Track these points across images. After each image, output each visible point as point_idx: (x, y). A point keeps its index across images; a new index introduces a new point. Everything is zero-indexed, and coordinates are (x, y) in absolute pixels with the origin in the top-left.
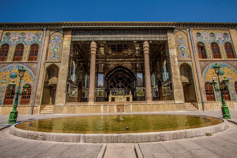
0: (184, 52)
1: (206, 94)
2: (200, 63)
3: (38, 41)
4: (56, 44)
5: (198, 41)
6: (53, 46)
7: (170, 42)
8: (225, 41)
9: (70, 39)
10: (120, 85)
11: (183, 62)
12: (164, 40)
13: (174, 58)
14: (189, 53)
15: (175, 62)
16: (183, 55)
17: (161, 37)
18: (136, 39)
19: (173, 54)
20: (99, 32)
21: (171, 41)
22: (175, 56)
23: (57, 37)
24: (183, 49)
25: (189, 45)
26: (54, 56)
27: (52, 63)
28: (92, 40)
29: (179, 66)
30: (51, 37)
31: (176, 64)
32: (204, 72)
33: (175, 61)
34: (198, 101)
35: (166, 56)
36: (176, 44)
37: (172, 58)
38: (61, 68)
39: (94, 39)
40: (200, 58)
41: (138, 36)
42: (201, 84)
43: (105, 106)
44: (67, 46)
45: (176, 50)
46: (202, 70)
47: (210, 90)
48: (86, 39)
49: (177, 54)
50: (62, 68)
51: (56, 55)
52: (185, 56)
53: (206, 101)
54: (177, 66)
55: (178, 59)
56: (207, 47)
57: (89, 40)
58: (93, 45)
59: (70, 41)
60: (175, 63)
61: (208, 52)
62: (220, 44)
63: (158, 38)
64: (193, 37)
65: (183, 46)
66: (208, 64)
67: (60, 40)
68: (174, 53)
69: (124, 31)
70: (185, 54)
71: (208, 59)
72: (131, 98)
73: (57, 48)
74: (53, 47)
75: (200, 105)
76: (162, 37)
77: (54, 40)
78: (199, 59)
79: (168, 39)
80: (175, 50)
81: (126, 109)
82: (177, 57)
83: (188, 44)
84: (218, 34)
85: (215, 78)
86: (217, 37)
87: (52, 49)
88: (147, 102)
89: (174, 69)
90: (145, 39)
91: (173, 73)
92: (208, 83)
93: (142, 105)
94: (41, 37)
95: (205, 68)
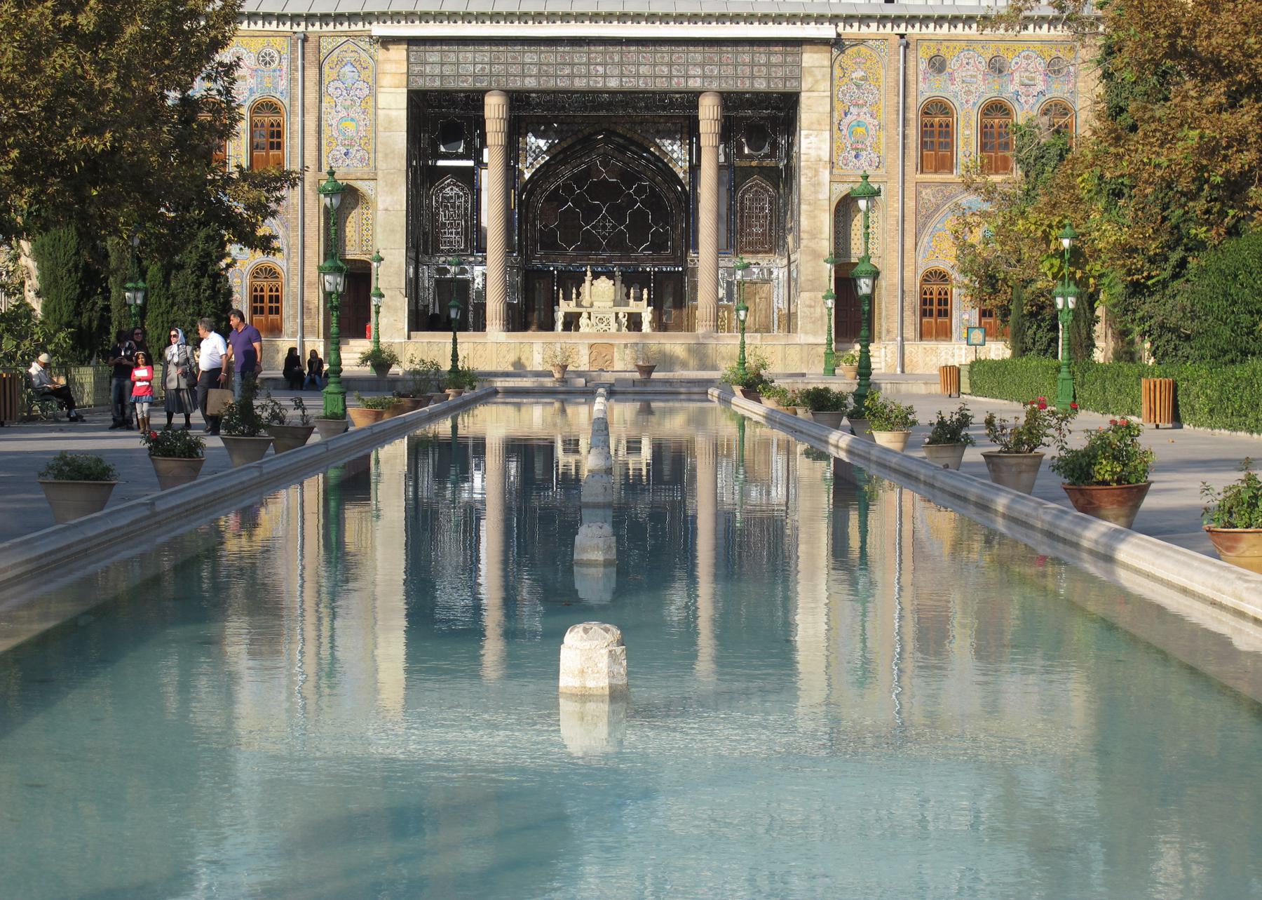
1: (918, 313)
4: (349, 102)
5: (927, 95)
6: (339, 108)
7: (809, 98)
8: (1047, 97)
9: (405, 83)
12: (787, 90)
13: (816, 171)
15: (816, 185)
17: (774, 75)
19: (813, 153)
21: (815, 94)
22: (820, 160)
23: (348, 68)
30: (326, 69)
31: (821, 197)
33: (819, 184)
37: (809, 168)
38: (381, 206)
44: (394, 113)
48: (466, 81)
51: (353, 151)
52: (862, 161)
56: (961, 124)
57: (478, 85)
60: (816, 192)
61: (961, 143)
62: (1022, 109)
65: (862, 118)
68: (820, 149)
70: (864, 153)
72: (647, 314)
73: (352, 119)
79: (804, 86)
84: (1025, 62)
86: (1017, 76)
87: (334, 122)
89: (813, 217)
91: (804, 232)
92: (936, 272)
94: (285, 69)
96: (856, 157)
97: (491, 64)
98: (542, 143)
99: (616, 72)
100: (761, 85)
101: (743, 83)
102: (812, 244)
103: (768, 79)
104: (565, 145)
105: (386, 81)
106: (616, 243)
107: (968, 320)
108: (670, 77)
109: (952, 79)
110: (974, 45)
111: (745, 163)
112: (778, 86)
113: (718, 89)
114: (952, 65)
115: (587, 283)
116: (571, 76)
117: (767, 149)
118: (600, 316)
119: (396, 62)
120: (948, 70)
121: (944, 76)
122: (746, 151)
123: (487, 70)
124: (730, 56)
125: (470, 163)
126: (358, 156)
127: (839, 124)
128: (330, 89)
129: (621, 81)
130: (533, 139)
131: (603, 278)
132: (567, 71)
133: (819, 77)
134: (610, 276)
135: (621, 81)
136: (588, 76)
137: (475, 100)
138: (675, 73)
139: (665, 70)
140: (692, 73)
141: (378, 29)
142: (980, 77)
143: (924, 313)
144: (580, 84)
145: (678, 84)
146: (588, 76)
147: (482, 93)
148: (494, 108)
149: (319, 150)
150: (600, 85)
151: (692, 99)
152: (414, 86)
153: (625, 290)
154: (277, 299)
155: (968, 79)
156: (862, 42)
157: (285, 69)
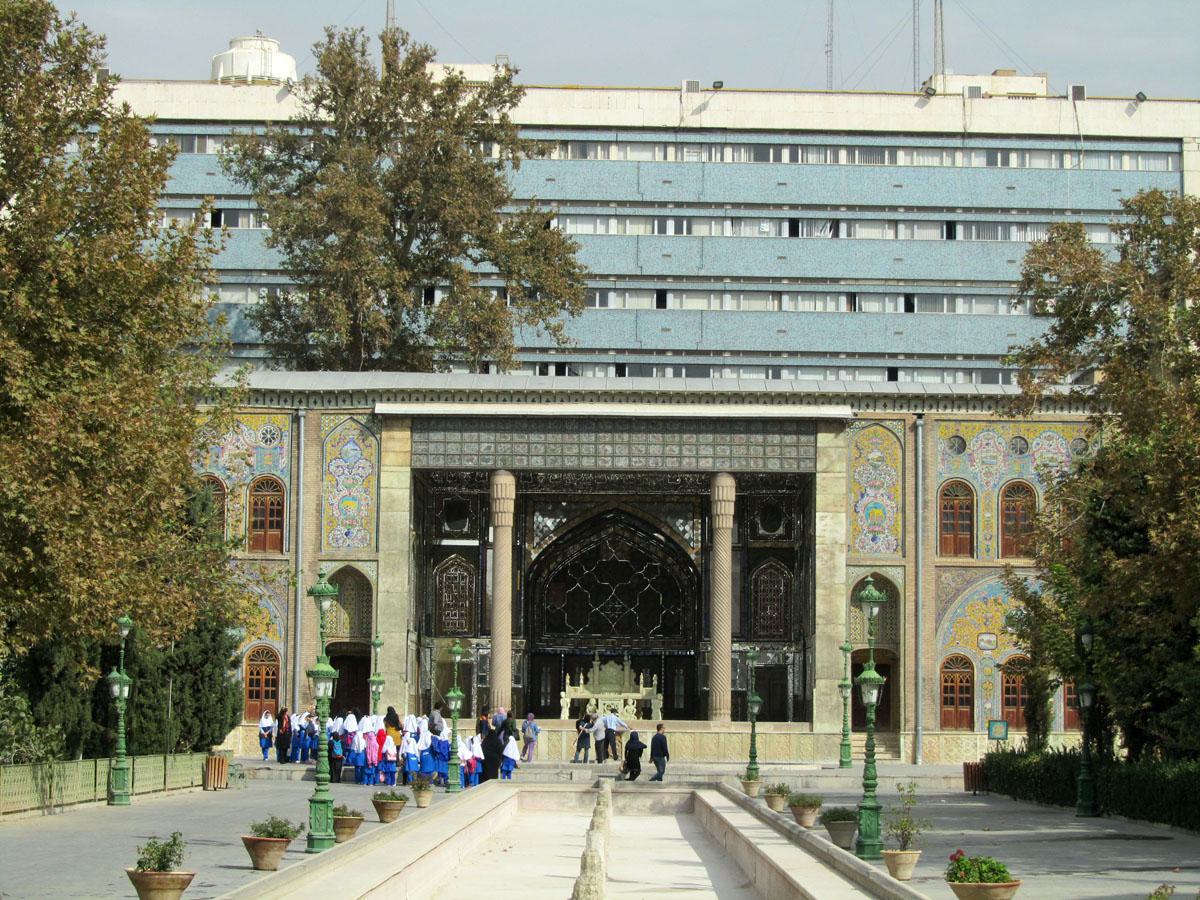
2: (939, 577)
3: (277, 466)
4: (350, 481)
5: (946, 476)
6: (341, 487)
7: (824, 479)
9: (408, 461)
12: (801, 470)
13: (832, 554)
14: (900, 529)
18: (680, 463)
21: (831, 475)
23: (351, 446)
24: (877, 511)
25: (904, 495)
26: (347, 534)
28: (500, 464)
30: (328, 447)
32: (948, 615)
36: (850, 490)
37: (824, 551)
39: (504, 461)
41: (690, 451)
42: (922, 661)
43: (554, 736)
44: (396, 493)
46: (944, 602)
47: (961, 687)
48: (472, 460)
49: (848, 531)
50: (387, 586)
51: (354, 531)
52: (880, 543)
54: (843, 587)
55: (847, 559)
57: (484, 464)
59: (409, 469)
60: (832, 576)
61: (981, 525)
63: (773, 457)
64: (929, 459)
65: (879, 500)
66: (969, 583)
67: (362, 463)
68: (836, 531)
69: (634, 427)
70: (881, 536)
72: (658, 703)
75: (906, 741)
76: (794, 455)
77: (340, 462)
82: (845, 549)
83: (904, 488)
84: (1046, 443)
85: (989, 642)
87: (335, 501)
88: (709, 727)
89: (828, 602)
90: (719, 466)
91: (820, 617)
92: (957, 659)
93: (687, 736)
94: (286, 446)
95: (956, 596)
96: (874, 539)
97: (495, 443)
98: (549, 523)
99: (625, 451)
100: (774, 466)
102: (828, 629)
103: (781, 459)
104: (573, 524)
105: (388, 459)
106: (626, 627)
107: (991, 710)
108: (680, 457)
109: (972, 461)
110: (994, 425)
111: (757, 545)
112: (791, 467)
113: (733, 469)
114: (971, 445)
115: (596, 668)
116: (579, 456)
117: (781, 531)
118: (608, 703)
119: (401, 440)
120: (967, 451)
121: (963, 457)
122: (761, 531)
123: (493, 449)
125: (476, 543)
126: (360, 535)
128: (332, 468)
129: (630, 461)
130: (540, 519)
131: (612, 662)
132: (575, 450)
133: (835, 457)
134: (619, 660)
135: (630, 461)
136: (596, 455)
137: (483, 479)
138: (685, 452)
139: (676, 449)
140: (703, 452)
141: (382, 408)
142: (1001, 458)
143: (946, 702)
144: (587, 463)
145: (690, 464)
146: (596, 455)
147: (492, 472)
148: (505, 488)
149: (319, 529)
150: (608, 465)
151: (708, 479)
152: (418, 465)
153: (634, 676)
154: (275, 683)
155: (988, 460)
156: (878, 422)
157: (286, 446)
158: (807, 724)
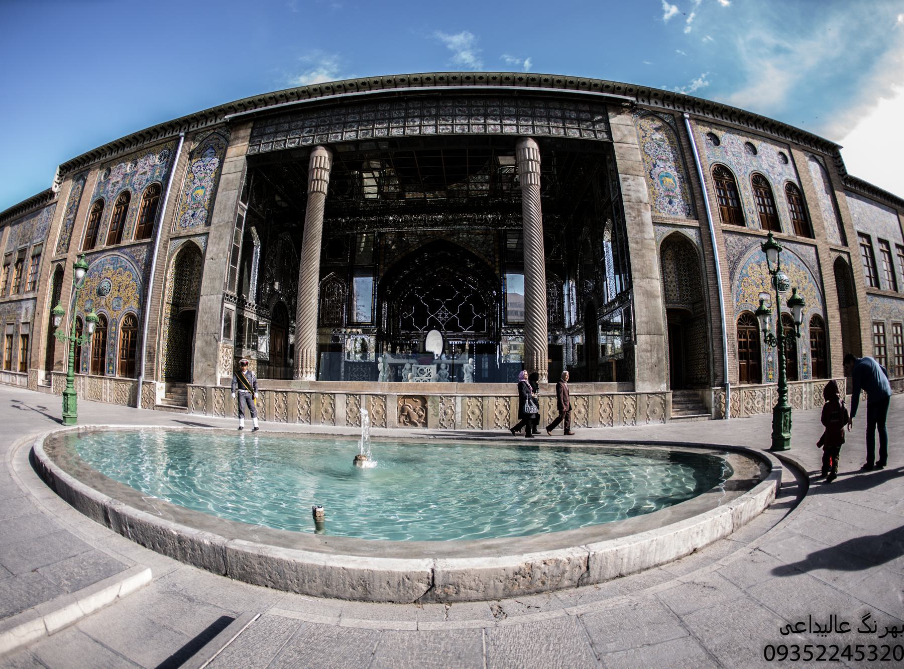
0: (673, 192)
1: (737, 356)
2: (726, 240)
6: (196, 181)
7: (621, 148)
10: (443, 316)
11: (670, 230)
13: (639, 211)
15: (641, 224)
16: (670, 202)
20: (343, 114)
22: (641, 202)
26: (193, 216)
27: (185, 240)
28: (317, 141)
29: (657, 242)
32: (737, 276)
33: (642, 223)
34: (712, 384)
35: (609, 202)
37: (631, 208)
40: (724, 221)
43: (352, 400)
45: (647, 182)
48: (294, 143)
51: (198, 212)
52: (676, 207)
53: (735, 384)
54: (654, 243)
55: (653, 217)
57: (304, 143)
58: (322, 158)
59: (244, 157)
60: (642, 232)
68: (638, 191)
71: (746, 228)
73: (203, 187)
74: (196, 185)
78: (723, 225)
80: (642, 180)
81: (437, 416)
96: (670, 202)
101: (557, 131)
124: (543, 111)
127: (650, 173)
158: (631, 383)
